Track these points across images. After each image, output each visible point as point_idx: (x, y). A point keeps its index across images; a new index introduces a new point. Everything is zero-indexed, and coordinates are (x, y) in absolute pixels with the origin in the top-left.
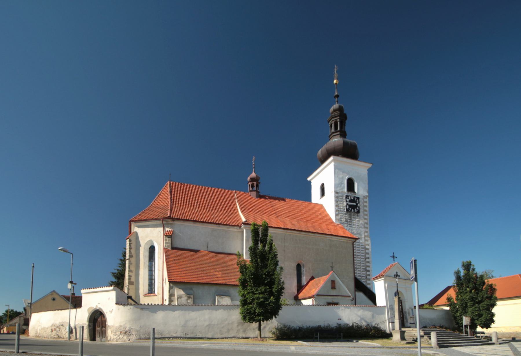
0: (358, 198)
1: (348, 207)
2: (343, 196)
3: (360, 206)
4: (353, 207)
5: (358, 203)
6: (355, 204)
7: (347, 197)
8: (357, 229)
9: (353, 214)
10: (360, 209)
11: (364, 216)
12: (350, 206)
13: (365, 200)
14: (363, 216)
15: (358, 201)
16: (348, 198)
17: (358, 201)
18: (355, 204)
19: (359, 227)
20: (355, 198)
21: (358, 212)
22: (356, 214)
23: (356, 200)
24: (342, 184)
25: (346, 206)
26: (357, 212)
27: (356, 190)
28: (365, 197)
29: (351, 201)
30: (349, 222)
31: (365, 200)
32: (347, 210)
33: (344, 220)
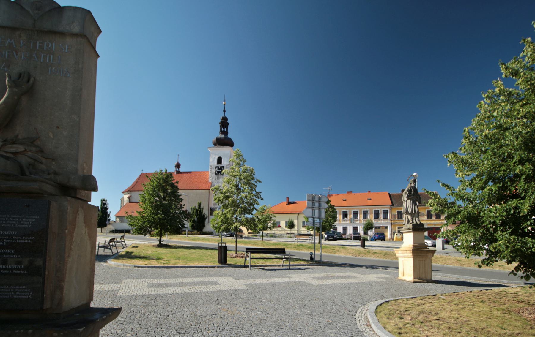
0: (223, 167)
1: (216, 172)
2: (214, 167)
4: (220, 172)
6: (220, 170)
7: (216, 167)
12: (218, 172)
13: (227, 167)
18: (220, 170)
22: (221, 175)
24: (214, 161)
27: (222, 163)
28: (227, 165)
29: (219, 169)
30: (217, 180)
32: (216, 174)
33: (214, 179)
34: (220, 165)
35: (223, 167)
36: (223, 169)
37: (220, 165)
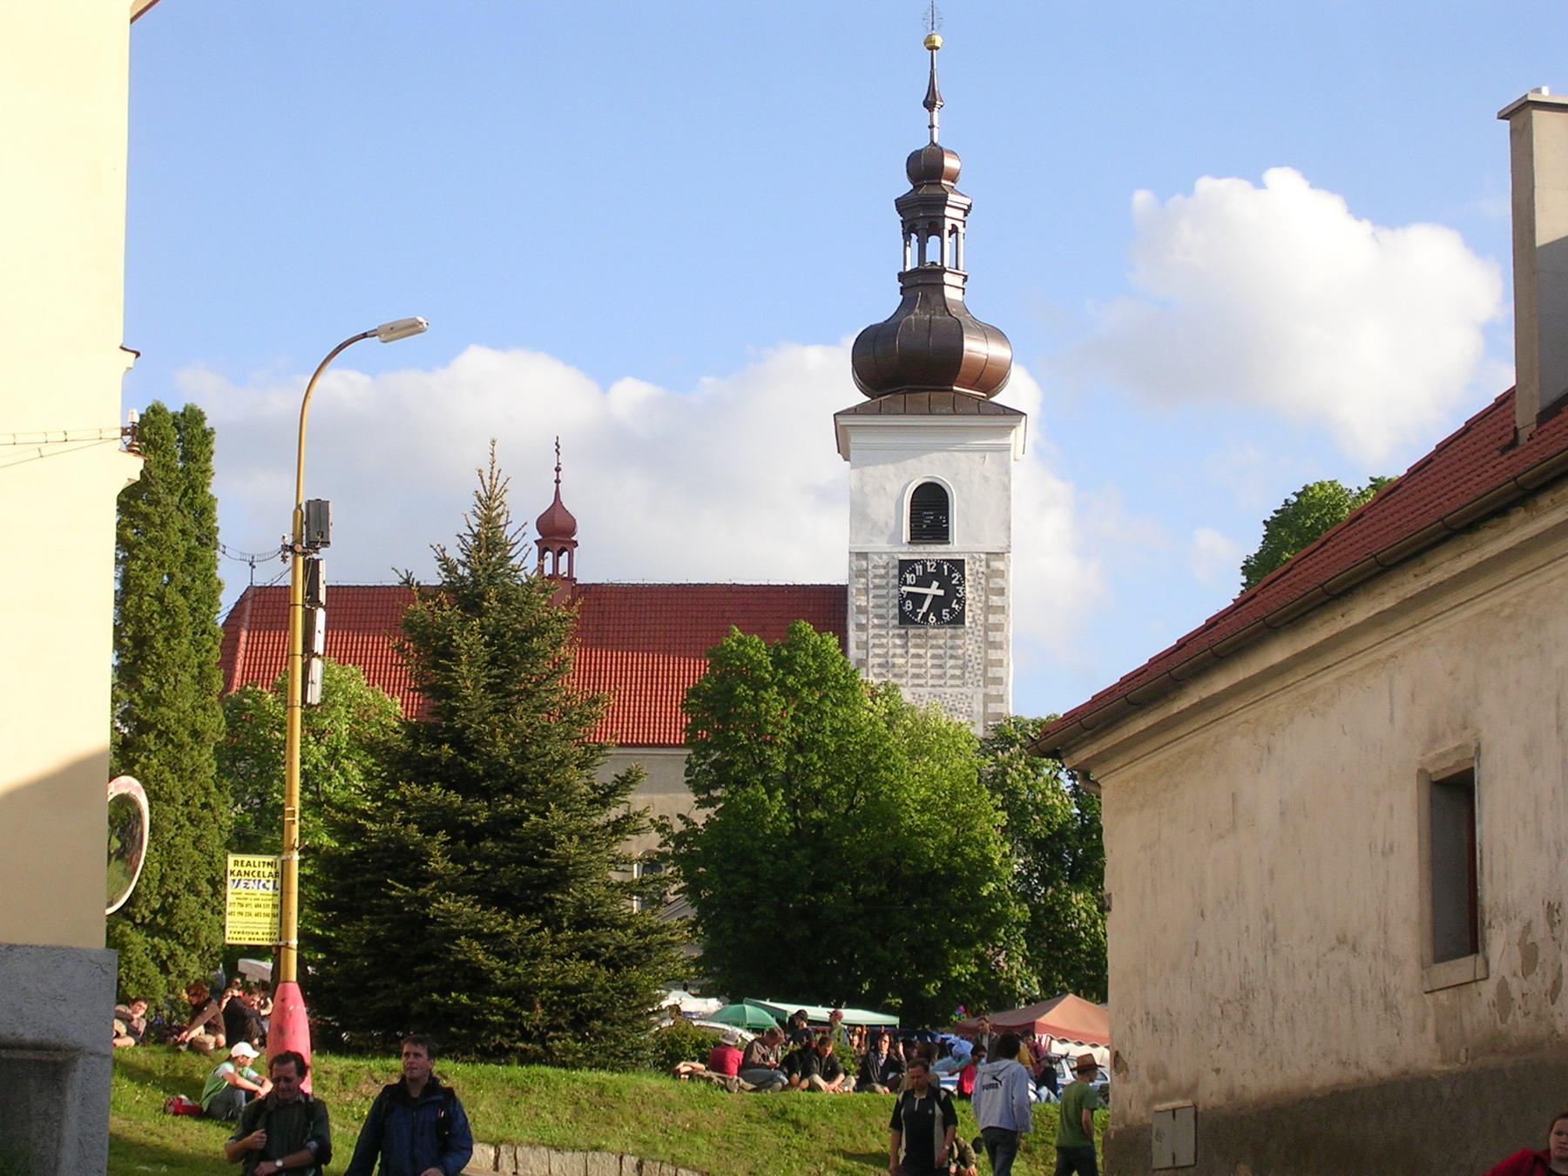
0: (958, 565)
3: (968, 595)
5: (960, 585)
7: (905, 566)
8: (952, 689)
9: (932, 632)
10: (967, 608)
11: (986, 633)
14: (982, 633)
15: (957, 575)
16: (914, 571)
17: (957, 575)
19: (959, 682)
20: (945, 567)
21: (958, 620)
22: (950, 631)
23: (950, 571)
25: (901, 606)
26: (948, 623)
31: (996, 564)
34: (933, 552)
35: (958, 565)
36: (961, 582)
37: (933, 552)
